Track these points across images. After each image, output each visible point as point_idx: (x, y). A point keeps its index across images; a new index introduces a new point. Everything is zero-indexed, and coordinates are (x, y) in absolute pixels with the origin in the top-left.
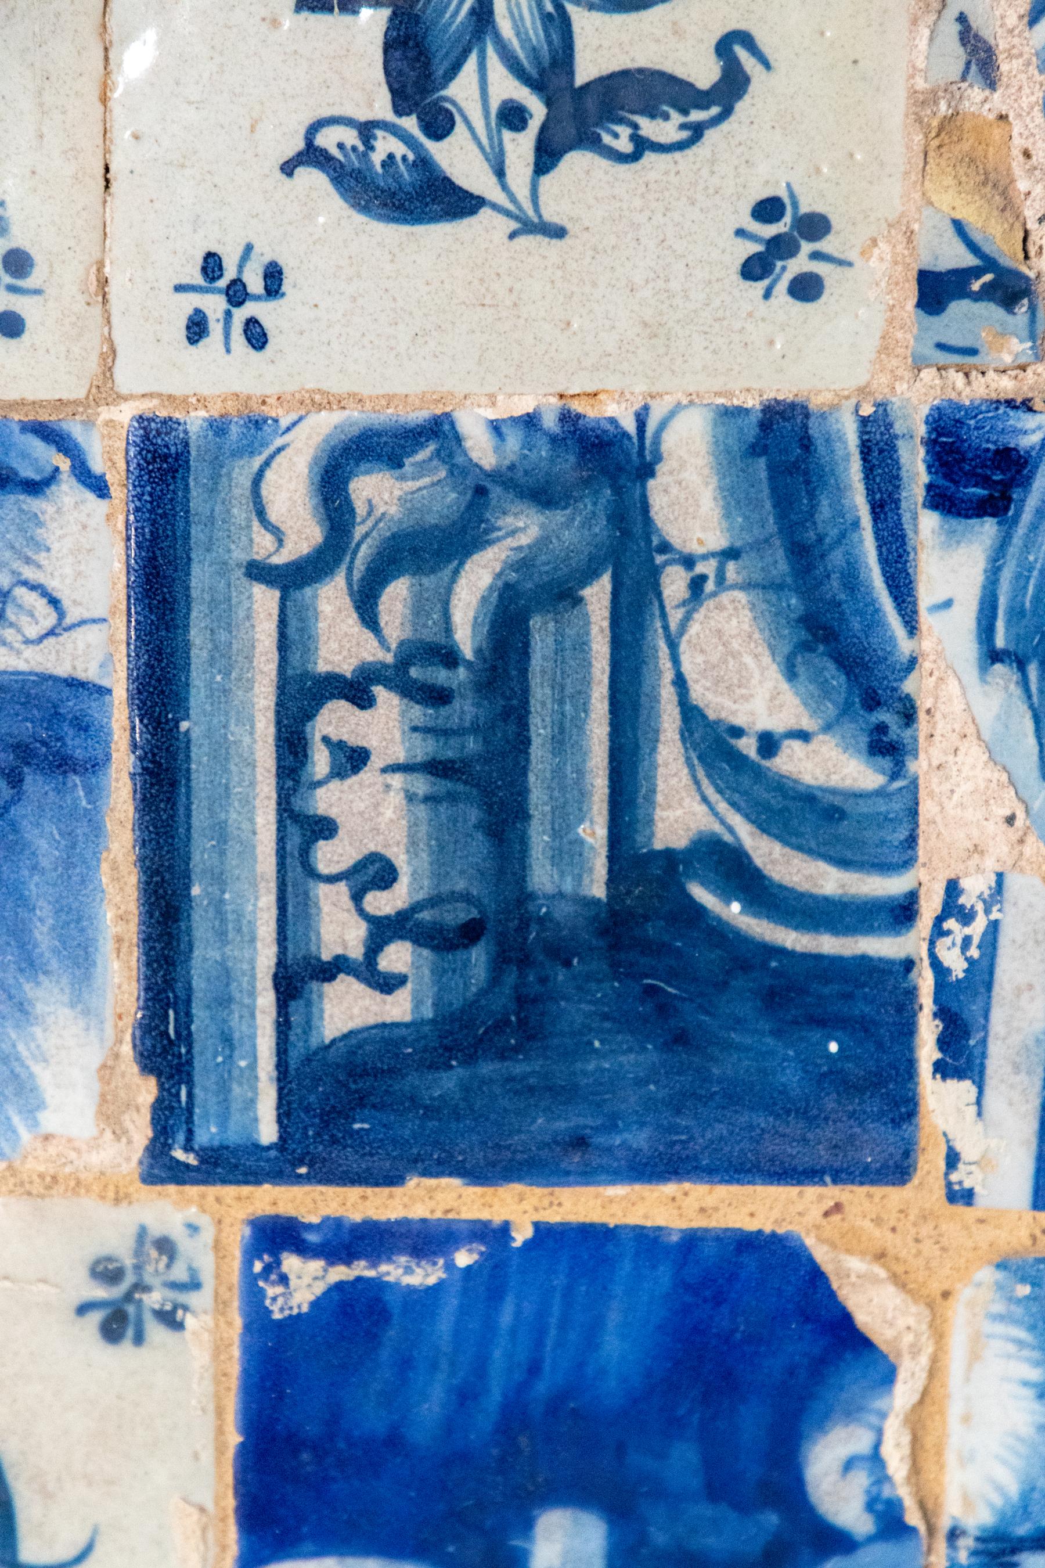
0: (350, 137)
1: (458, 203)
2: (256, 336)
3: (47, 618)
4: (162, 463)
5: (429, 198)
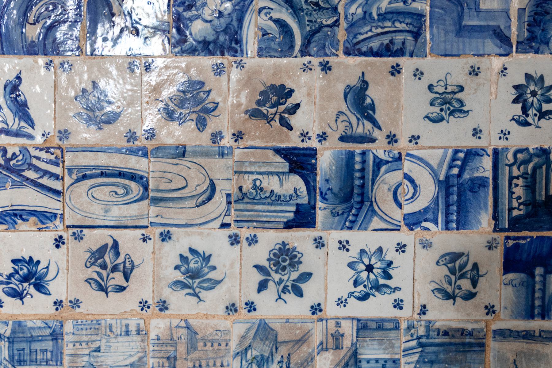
0: (518, 117)
1: (529, 124)
2: (507, 139)
3: (483, 170)
4: (496, 152)
5: (527, 124)
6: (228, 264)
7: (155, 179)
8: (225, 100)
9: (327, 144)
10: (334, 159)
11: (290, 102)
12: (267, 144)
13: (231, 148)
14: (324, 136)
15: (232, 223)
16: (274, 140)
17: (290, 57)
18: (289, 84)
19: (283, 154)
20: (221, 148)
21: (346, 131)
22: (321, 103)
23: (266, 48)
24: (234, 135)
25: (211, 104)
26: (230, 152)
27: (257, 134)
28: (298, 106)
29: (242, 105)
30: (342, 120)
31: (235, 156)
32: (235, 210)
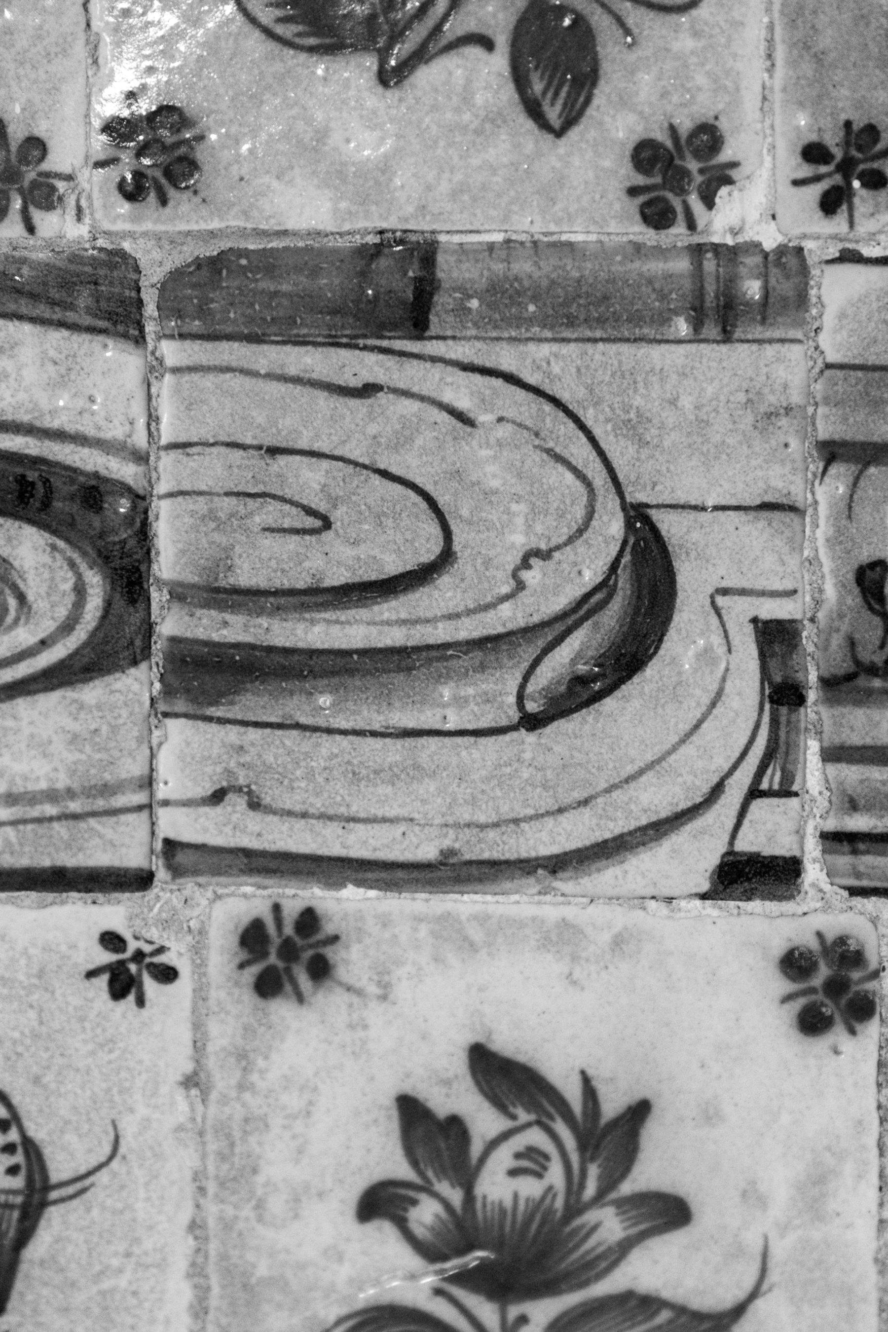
6: (780, 1182)
7: (201, 505)
13: (790, 261)
15: (812, 849)
20: (710, 264)
24: (814, 153)
31: (829, 320)
32: (834, 754)
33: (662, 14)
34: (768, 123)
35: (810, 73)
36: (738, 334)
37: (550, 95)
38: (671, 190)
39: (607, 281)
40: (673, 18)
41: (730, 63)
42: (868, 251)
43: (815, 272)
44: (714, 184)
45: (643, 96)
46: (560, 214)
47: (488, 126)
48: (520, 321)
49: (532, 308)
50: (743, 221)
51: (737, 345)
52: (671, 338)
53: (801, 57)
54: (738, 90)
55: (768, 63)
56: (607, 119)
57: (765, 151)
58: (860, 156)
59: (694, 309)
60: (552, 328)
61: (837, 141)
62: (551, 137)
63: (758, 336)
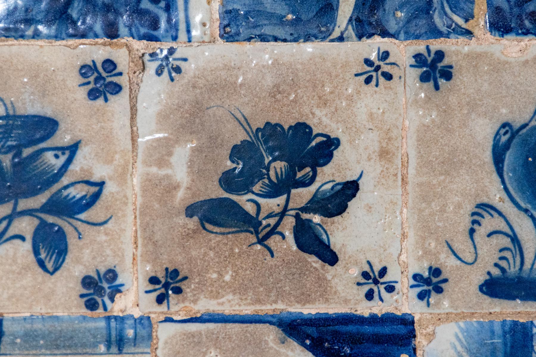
8: (122, 176)
9: (446, 303)
10: (468, 351)
11: (329, 176)
12: (258, 307)
13: (145, 322)
14: (435, 280)
16: (281, 295)
17: (323, 39)
18: (323, 122)
19: (308, 337)
20: (113, 324)
21: (504, 264)
22: (424, 179)
23: (247, 13)
24: (153, 280)
25: (79, 186)
26: (143, 332)
27: (227, 278)
28: (351, 189)
29: (177, 187)
30: (490, 229)
31: (161, 345)
33: (92, 226)
34: (135, 268)
35: (151, 249)
36: (125, 351)
37: (48, 259)
38: (97, 295)
39: (72, 331)
40: (97, 228)
41: (120, 246)
42: (175, 318)
43: (155, 326)
44: (114, 293)
45: (85, 259)
46: (52, 306)
47: (23, 271)
48: (36, 347)
49: (42, 342)
50: (126, 307)
51: (125, 355)
52: (98, 353)
53: (148, 243)
54: (123, 256)
55: (135, 246)
56: (71, 268)
57: (134, 280)
58: (171, 281)
59: (107, 341)
60: (50, 349)
61: (162, 275)
62: (49, 275)
63: (132, 352)
